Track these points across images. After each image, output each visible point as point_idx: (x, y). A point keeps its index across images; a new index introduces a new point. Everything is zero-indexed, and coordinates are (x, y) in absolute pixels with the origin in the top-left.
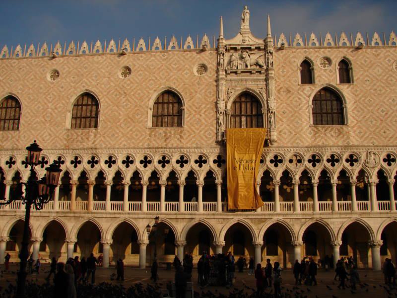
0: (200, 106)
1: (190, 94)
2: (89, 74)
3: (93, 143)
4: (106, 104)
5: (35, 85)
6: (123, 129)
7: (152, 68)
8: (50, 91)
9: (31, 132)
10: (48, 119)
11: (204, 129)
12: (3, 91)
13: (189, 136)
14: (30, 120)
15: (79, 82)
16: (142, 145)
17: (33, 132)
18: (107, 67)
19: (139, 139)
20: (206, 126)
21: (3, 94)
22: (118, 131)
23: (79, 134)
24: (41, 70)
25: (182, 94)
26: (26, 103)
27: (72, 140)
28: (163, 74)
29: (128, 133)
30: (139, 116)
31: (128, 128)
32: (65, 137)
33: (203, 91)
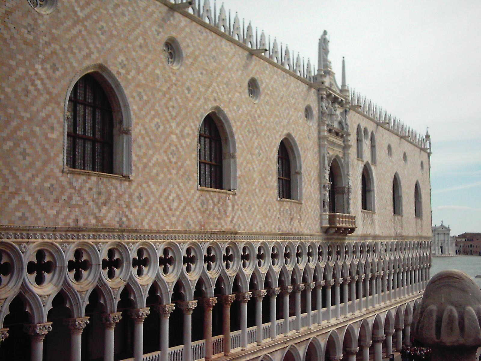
0: (311, 172)
1: (304, 152)
2: (219, 74)
3: (231, 222)
4: (240, 146)
5: (147, 66)
6: (258, 198)
7: (276, 94)
8: (172, 92)
9: (149, 186)
10: (174, 160)
11: (313, 207)
12: (88, 55)
13: (305, 216)
14: (145, 154)
15: (209, 87)
16: (274, 229)
17: (153, 187)
18: (237, 70)
19: (271, 217)
20: (315, 203)
21: (87, 63)
22: (254, 202)
23: (216, 200)
24: (153, 29)
25: (299, 148)
26: (135, 107)
27: (208, 212)
28: (285, 110)
29: (262, 205)
30: (271, 177)
31: (262, 196)
32: (199, 203)
33: (312, 150)
